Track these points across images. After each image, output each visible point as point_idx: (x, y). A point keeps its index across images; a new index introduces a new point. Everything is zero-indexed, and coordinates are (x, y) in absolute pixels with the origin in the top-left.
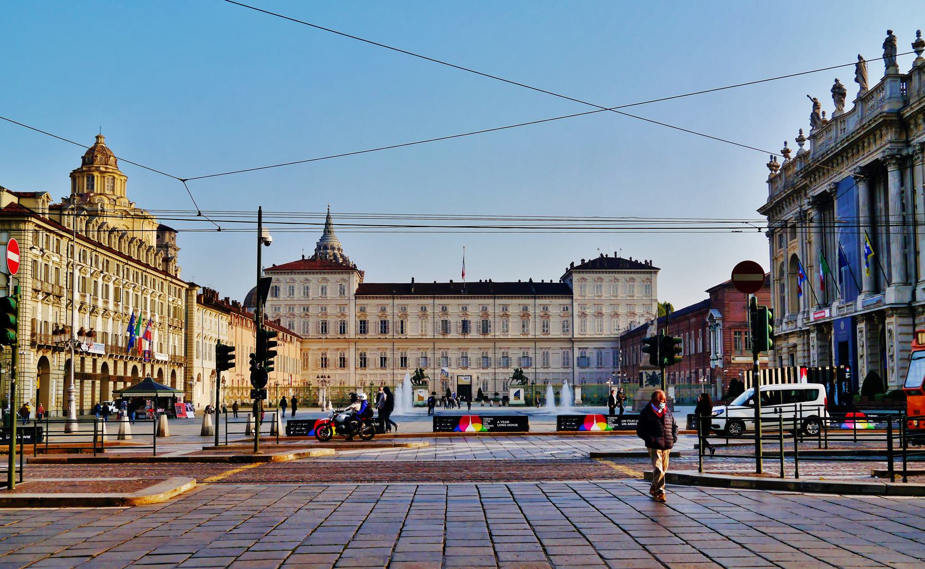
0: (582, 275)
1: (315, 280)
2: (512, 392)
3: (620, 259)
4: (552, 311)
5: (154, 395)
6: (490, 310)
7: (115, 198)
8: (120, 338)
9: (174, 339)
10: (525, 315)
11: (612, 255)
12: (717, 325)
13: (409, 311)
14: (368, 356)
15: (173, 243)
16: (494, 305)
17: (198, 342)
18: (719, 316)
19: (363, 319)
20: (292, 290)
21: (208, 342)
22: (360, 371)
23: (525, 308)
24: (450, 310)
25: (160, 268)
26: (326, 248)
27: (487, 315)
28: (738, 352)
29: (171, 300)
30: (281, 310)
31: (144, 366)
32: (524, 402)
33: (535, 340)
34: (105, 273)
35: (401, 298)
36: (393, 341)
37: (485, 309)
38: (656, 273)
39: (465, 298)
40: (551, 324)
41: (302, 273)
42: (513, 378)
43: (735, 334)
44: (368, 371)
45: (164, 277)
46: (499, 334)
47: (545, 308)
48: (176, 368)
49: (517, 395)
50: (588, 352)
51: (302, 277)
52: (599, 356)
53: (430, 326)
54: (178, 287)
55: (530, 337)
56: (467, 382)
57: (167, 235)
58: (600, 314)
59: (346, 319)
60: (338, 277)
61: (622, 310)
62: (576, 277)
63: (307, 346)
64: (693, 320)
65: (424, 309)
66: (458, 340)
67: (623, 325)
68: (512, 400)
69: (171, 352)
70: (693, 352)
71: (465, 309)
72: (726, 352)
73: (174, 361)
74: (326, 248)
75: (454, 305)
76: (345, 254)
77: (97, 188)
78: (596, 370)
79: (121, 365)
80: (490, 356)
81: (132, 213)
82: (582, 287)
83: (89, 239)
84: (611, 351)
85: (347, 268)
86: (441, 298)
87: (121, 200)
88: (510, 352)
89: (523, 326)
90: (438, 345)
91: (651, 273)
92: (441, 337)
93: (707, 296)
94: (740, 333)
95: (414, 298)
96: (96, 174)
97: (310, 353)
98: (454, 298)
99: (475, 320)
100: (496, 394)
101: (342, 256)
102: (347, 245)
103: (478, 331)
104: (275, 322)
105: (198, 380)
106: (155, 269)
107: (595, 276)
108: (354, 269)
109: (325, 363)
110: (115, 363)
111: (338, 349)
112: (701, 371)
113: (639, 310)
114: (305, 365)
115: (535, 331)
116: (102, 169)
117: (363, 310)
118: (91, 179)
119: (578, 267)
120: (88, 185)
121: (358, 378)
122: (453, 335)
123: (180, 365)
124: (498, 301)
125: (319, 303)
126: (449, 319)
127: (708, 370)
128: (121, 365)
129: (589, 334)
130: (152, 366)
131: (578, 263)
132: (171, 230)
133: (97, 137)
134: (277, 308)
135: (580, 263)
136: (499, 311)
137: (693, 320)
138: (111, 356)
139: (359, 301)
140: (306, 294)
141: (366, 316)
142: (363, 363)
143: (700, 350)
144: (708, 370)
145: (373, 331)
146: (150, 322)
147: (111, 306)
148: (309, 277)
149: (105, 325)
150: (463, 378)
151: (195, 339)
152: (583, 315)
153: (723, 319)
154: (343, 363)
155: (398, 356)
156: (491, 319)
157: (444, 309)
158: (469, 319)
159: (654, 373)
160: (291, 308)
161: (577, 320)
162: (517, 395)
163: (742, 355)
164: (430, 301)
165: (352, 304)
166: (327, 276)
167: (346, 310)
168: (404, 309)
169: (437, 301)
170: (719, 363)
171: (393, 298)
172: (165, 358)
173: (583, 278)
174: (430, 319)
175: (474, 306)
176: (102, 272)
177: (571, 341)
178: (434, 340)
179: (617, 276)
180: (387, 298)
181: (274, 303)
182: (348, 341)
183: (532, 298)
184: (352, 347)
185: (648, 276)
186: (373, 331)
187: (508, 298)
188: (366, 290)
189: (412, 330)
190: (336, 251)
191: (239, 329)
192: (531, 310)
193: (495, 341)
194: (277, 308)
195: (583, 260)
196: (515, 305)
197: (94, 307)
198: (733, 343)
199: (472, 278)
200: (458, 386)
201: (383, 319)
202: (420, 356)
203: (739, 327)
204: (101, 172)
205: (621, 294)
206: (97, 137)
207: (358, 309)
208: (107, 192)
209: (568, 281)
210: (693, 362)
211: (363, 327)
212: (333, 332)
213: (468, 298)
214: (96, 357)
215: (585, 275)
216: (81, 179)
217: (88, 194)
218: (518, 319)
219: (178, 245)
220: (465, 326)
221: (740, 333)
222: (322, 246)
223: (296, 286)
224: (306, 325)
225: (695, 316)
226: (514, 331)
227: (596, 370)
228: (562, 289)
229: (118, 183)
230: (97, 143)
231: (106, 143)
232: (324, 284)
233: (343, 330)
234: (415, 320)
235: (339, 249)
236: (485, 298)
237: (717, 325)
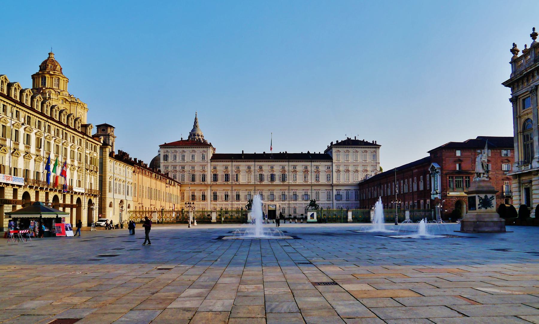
0: (338, 149)
1: (188, 151)
2: (309, 214)
3: (358, 140)
4: (321, 169)
5: (38, 216)
6: (286, 168)
7: (59, 91)
8: (41, 175)
9: (91, 179)
10: (306, 171)
11: (353, 138)
12: (438, 172)
13: (241, 168)
14: (218, 194)
15: (112, 133)
16: (288, 166)
17: (110, 182)
18: (439, 167)
19: (215, 173)
20: (175, 157)
21: (118, 182)
22: (213, 202)
23: (306, 167)
24: (264, 168)
25: (80, 130)
26: (194, 135)
27: (285, 171)
28: (451, 190)
29: (88, 152)
30: (169, 168)
31: (64, 196)
32: (316, 220)
33: (311, 185)
34: (26, 125)
35: (236, 161)
36: (232, 186)
37: (283, 168)
38: (379, 148)
39: (272, 161)
40: (320, 177)
41: (181, 147)
42: (310, 205)
43: (450, 178)
44: (218, 202)
45: (82, 136)
46: (291, 182)
47: (317, 167)
48: (92, 198)
49: (312, 216)
50: (341, 191)
51: (181, 150)
52: (347, 194)
53: (252, 177)
54: (94, 145)
55: (308, 183)
56: (273, 208)
57: (109, 129)
58: (348, 171)
59: (206, 173)
60: (201, 150)
61: (360, 169)
62: (334, 150)
63: (183, 188)
64: (416, 170)
65: (249, 167)
66: (268, 185)
67: (360, 177)
68: (309, 219)
69: (88, 187)
70: (415, 189)
71: (272, 167)
72: (444, 189)
73: (90, 193)
74: (194, 135)
75: (266, 166)
76: (205, 139)
77: (48, 85)
78: (345, 202)
79: (42, 195)
80: (286, 194)
81: (70, 100)
82: (338, 156)
83: (11, 98)
84: (354, 192)
85: (205, 145)
86: (259, 161)
87: (63, 92)
88: (298, 192)
89: (305, 177)
90: (257, 188)
91: (376, 148)
93: (428, 155)
94: (452, 178)
95: (244, 161)
96: (47, 76)
97: (185, 192)
98: (266, 161)
99: (278, 174)
100: (290, 215)
101: (203, 140)
102: (206, 133)
103: (280, 180)
104: (165, 174)
105: (110, 206)
106: (75, 130)
107: (345, 149)
108: (210, 145)
109: (193, 197)
110: (37, 193)
111: (201, 190)
112: (422, 201)
113: (369, 168)
114: (183, 199)
115: (311, 180)
116: (51, 73)
117: (215, 168)
118: (44, 79)
119: (335, 145)
120: (42, 83)
121: (212, 206)
122: (265, 182)
123: (95, 196)
124: (291, 163)
125: (190, 164)
126: (263, 173)
127: (428, 201)
128: (42, 195)
129: (342, 182)
130: (72, 197)
131: (335, 143)
132: (111, 127)
133: (49, 54)
135: (335, 143)
136: (291, 169)
137: (416, 170)
138: (31, 187)
139: (213, 163)
140: (183, 159)
141: (216, 171)
142: (215, 197)
143: (421, 188)
144: (428, 201)
146: (65, 164)
147: (33, 150)
148: (185, 149)
149: (27, 164)
150: (271, 206)
151: (108, 180)
152: (338, 171)
153: (442, 169)
154: (204, 198)
155: (235, 194)
156: (286, 173)
157: (261, 168)
158: (275, 173)
159: (486, 197)
160: (175, 167)
161: (335, 174)
162: (312, 216)
163: (454, 191)
164: (253, 163)
165: (209, 165)
166: (195, 149)
167: (206, 168)
168: (238, 167)
169: (257, 163)
170: (438, 196)
171: (232, 161)
172: (82, 190)
173: (338, 151)
174: (253, 173)
175: (277, 166)
176: (23, 124)
177: (332, 185)
178: (255, 185)
179: (357, 149)
180: (229, 161)
181: (165, 164)
182: (206, 185)
183: (310, 161)
184: (209, 189)
185: (374, 149)
186: (220, 180)
187: (297, 161)
188: (217, 157)
189: (243, 179)
190: (200, 137)
191: (140, 176)
192: (309, 169)
193: (289, 185)
194: (166, 167)
195: (337, 141)
196: (300, 166)
197: (15, 150)
198: (448, 184)
199: (276, 151)
200: (269, 211)
201: (226, 173)
202: (247, 194)
203: (452, 173)
204: (51, 75)
205: (360, 160)
206: (49, 54)
207: (212, 168)
208: (54, 87)
209: (329, 153)
210: (416, 196)
213: (274, 161)
214: (16, 187)
215: (340, 149)
216: (38, 79)
217: (41, 89)
218: (302, 174)
219: (115, 135)
220: (272, 178)
221: (452, 178)
222: (193, 134)
223: (178, 154)
224: (183, 176)
225: (417, 168)
226: (300, 180)
227: (345, 202)
228: (327, 156)
229: (62, 82)
230: (49, 57)
231: (55, 57)
232: (193, 154)
233: (204, 179)
234: (244, 174)
235: (202, 136)
236: (283, 161)
237: (438, 172)
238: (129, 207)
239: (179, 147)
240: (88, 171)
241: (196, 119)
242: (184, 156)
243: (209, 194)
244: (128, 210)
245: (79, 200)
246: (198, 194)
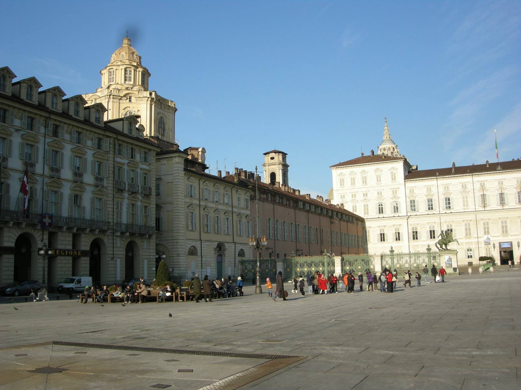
53: (470, 201)
65: (464, 186)
117: (412, 191)
134: (343, 197)
140: (365, 182)
194: (343, 197)
211: (413, 205)
233: (396, 209)
238: (242, 253)
240: (126, 195)
244: (240, 258)
245: (96, 245)
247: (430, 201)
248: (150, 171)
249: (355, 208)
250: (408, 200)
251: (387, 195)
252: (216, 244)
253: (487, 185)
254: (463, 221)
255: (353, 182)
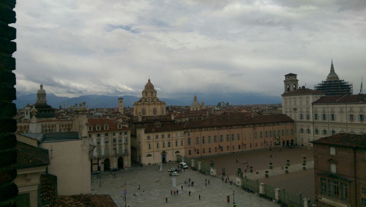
36: (328, 123)
41: (293, 95)
92: (350, 122)
97: (297, 126)
139: (314, 106)
140: (295, 104)
142: (317, 132)
145: (320, 119)
148: (296, 97)
165: (311, 107)
178: (347, 124)
186: (320, 119)
207: (314, 109)
212: (305, 119)
233: (308, 118)
239: (292, 96)
241: (332, 65)
242: (295, 101)
243: (311, 129)
246: (305, 129)
247: (324, 115)
248: (127, 137)
249: (291, 115)
250: (314, 114)
251: (304, 110)
252: (162, 152)
253: (354, 110)
254: (340, 127)
255: (290, 102)
